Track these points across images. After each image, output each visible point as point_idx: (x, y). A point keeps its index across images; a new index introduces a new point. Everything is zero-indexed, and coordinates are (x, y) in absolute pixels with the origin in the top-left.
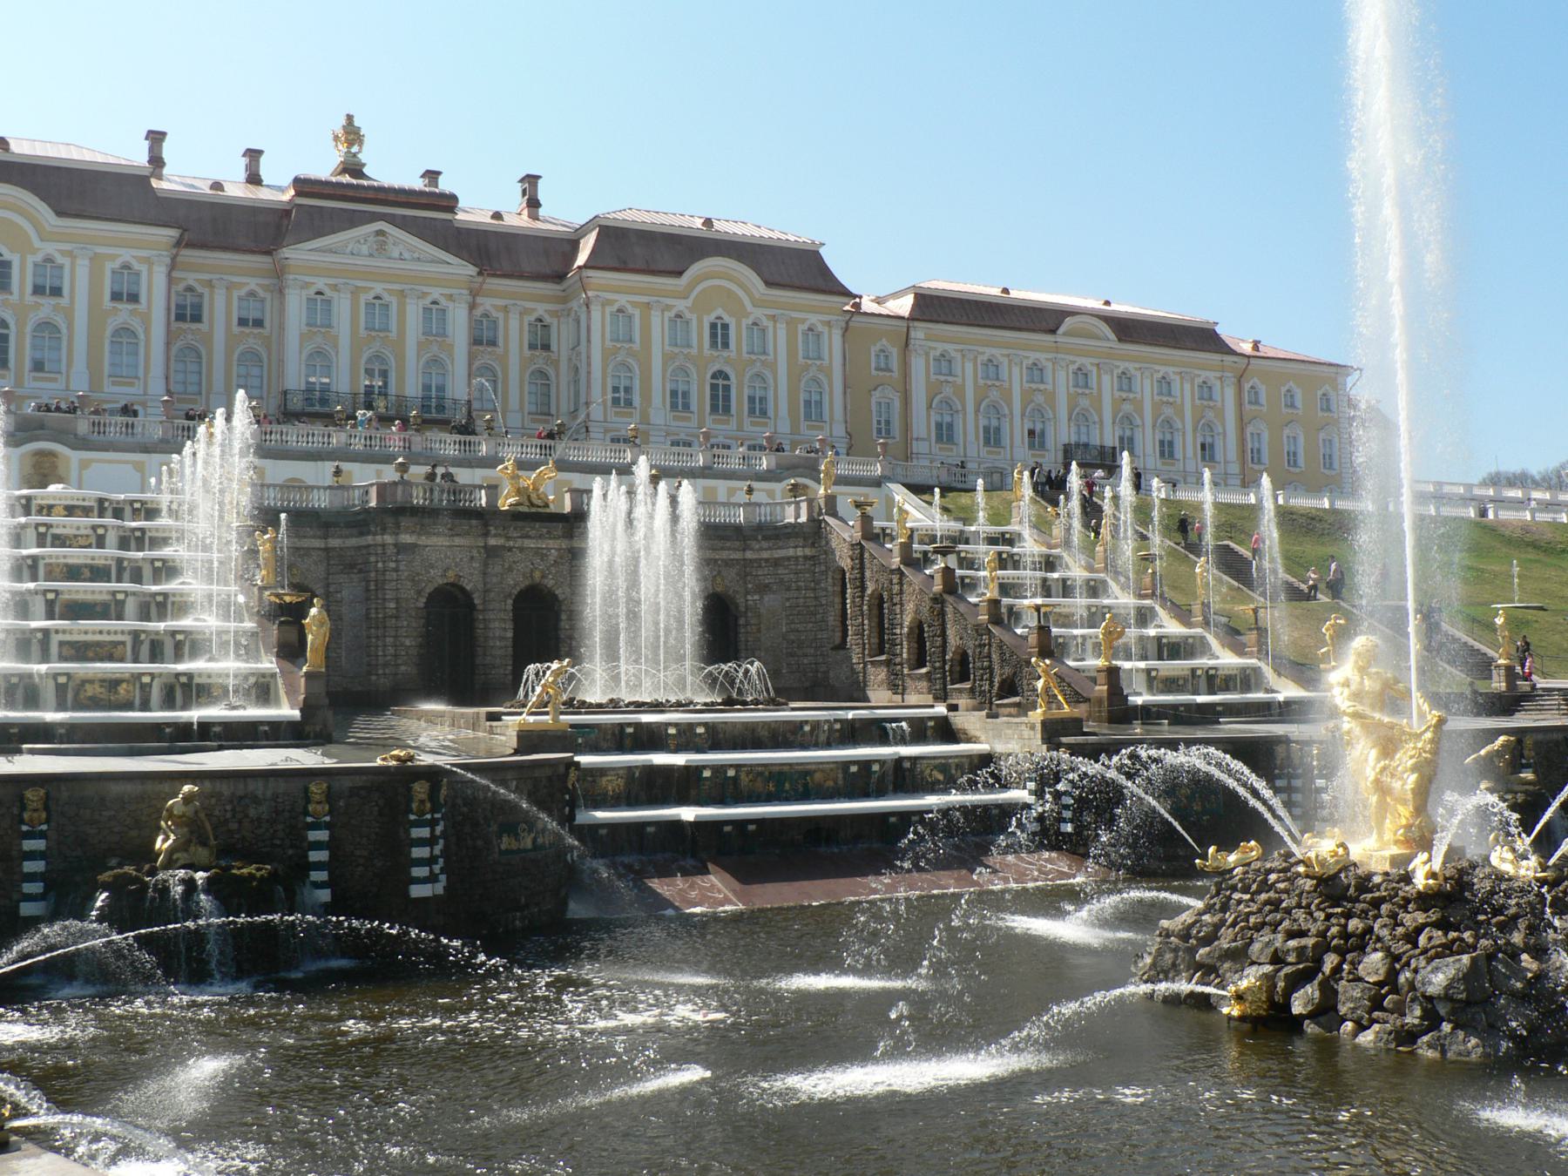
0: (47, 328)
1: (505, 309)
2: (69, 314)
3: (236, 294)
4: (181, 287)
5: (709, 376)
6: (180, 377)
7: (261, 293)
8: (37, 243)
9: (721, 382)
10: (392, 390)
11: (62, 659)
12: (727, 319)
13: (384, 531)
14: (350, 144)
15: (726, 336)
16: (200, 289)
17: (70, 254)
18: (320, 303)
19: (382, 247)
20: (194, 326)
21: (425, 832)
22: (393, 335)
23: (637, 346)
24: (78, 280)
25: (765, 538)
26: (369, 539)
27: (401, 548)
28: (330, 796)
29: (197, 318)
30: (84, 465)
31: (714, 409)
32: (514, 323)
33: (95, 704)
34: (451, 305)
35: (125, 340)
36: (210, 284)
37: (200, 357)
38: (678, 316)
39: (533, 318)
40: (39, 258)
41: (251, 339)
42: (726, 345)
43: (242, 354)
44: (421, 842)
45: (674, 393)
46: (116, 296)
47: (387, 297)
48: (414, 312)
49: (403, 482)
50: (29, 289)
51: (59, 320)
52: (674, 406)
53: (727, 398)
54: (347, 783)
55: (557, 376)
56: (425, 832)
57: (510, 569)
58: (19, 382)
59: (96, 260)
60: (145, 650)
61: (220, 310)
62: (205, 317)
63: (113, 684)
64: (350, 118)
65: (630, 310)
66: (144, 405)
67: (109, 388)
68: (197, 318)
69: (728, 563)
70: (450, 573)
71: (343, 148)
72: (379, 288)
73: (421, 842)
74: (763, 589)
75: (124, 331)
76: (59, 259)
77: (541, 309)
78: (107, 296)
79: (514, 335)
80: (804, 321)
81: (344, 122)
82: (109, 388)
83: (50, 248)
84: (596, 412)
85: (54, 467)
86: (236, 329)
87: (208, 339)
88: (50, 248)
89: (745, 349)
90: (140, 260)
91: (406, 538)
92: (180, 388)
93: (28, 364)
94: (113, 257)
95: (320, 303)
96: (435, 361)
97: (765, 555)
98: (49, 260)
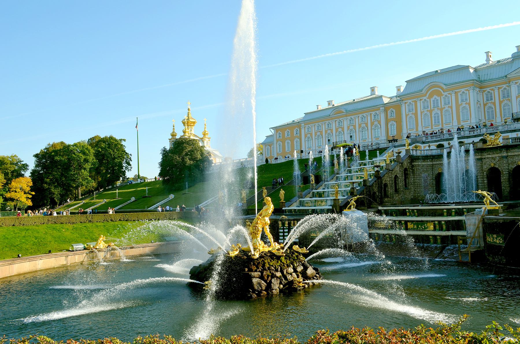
2: (451, 107)
8: (443, 93)
21: (282, 231)
43: (504, 106)
44: (281, 232)
50: (443, 104)
56: (282, 231)
57: (485, 164)
73: (281, 232)
76: (448, 95)
78: (460, 101)
82: (462, 124)
83: (446, 93)
87: (494, 104)
90: (466, 90)
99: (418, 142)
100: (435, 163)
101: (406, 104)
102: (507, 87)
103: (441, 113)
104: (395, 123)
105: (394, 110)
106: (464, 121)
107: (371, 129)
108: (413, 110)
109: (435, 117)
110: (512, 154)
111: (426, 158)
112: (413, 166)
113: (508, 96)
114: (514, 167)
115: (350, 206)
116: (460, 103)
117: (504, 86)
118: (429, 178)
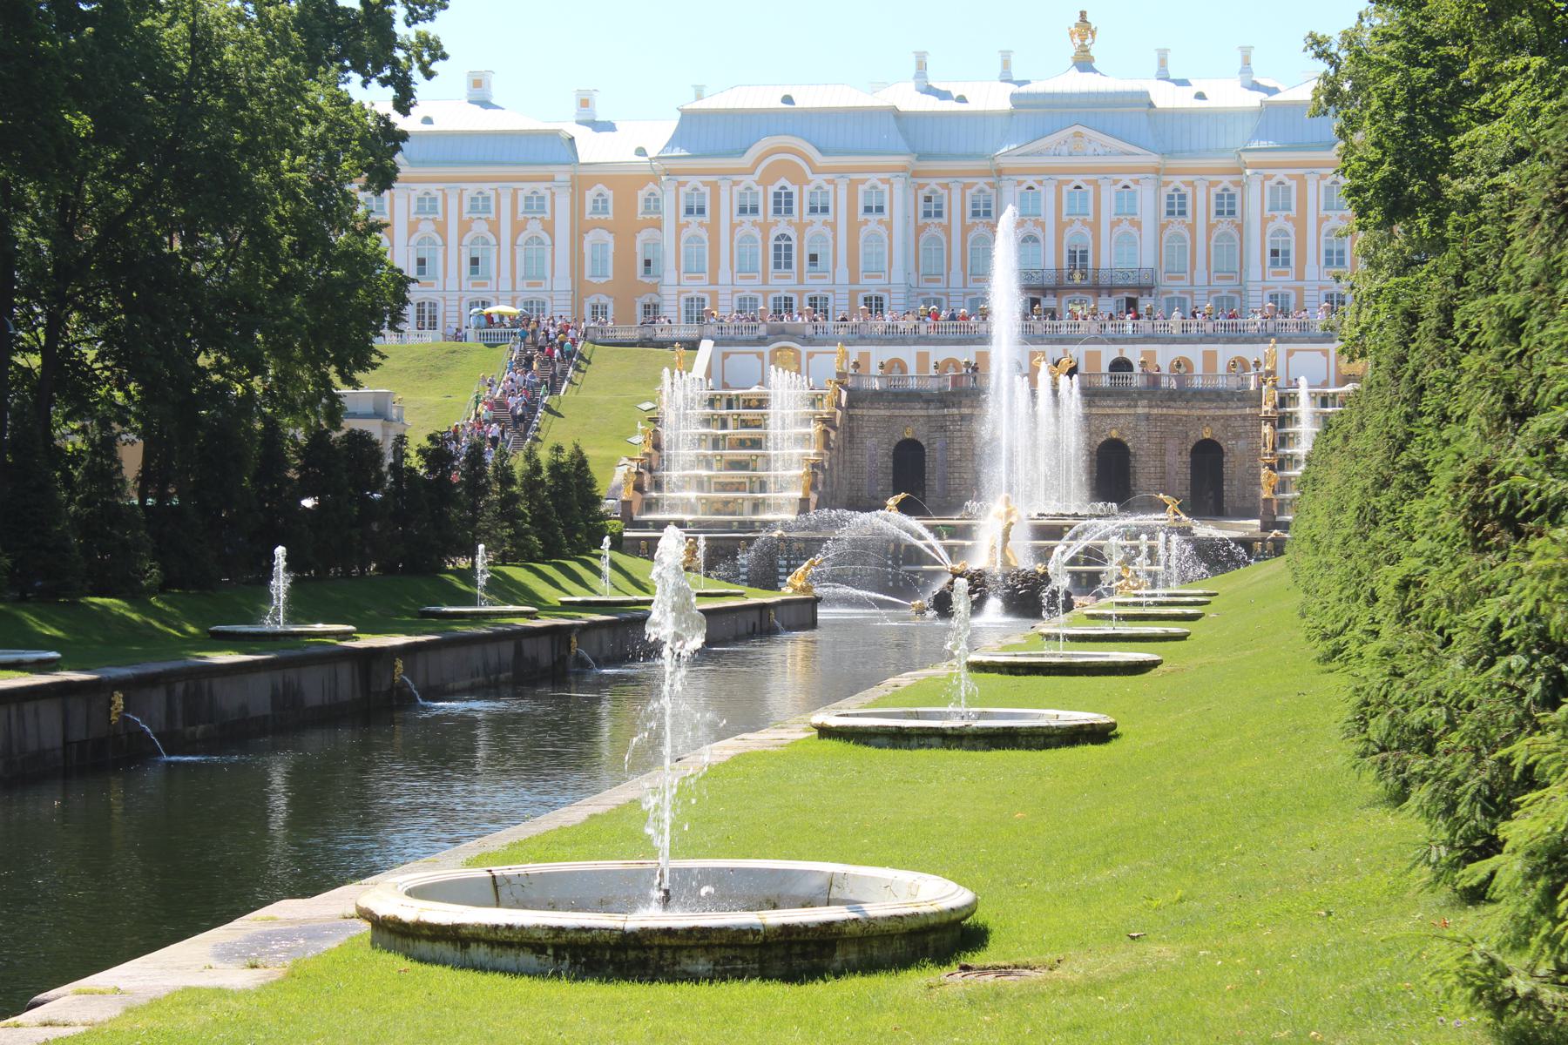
1: (1191, 184)
2: (834, 226)
3: (968, 192)
4: (926, 191)
10: (1090, 264)
16: (940, 191)
17: (829, 182)
20: (937, 220)
22: (1090, 218)
23: (1293, 213)
29: (939, 214)
30: (810, 355)
34: (1138, 188)
36: (946, 187)
39: (1218, 190)
40: (811, 187)
45: (1329, 252)
46: (868, 209)
48: (1108, 194)
50: (806, 208)
52: (1329, 262)
58: (801, 282)
59: (853, 186)
60: (757, 486)
63: (726, 503)
64: (1083, 14)
65: (1288, 182)
66: (889, 291)
67: (863, 281)
68: (939, 214)
69: (1214, 418)
71: (1077, 40)
72: (1078, 180)
74: (1237, 436)
76: (826, 187)
77: (1226, 181)
78: (861, 209)
79: (1201, 203)
81: (1077, 19)
83: (819, 179)
84: (1254, 273)
86: (969, 221)
87: (947, 230)
90: (884, 181)
91: (965, 411)
94: (863, 182)
97: (1239, 412)
98: (819, 187)
100: (897, 412)
101: (682, 190)
102: (986, 188)
103: (800, 239)
107: (514, 244)
108: (701, 211)
109: (777, 248)
110: (1101, 411)
111: (877, 397)
112: (851, 418)
113: (987, 214)
116: (861, 216)
117: (981, 183)
118: (880, 452)
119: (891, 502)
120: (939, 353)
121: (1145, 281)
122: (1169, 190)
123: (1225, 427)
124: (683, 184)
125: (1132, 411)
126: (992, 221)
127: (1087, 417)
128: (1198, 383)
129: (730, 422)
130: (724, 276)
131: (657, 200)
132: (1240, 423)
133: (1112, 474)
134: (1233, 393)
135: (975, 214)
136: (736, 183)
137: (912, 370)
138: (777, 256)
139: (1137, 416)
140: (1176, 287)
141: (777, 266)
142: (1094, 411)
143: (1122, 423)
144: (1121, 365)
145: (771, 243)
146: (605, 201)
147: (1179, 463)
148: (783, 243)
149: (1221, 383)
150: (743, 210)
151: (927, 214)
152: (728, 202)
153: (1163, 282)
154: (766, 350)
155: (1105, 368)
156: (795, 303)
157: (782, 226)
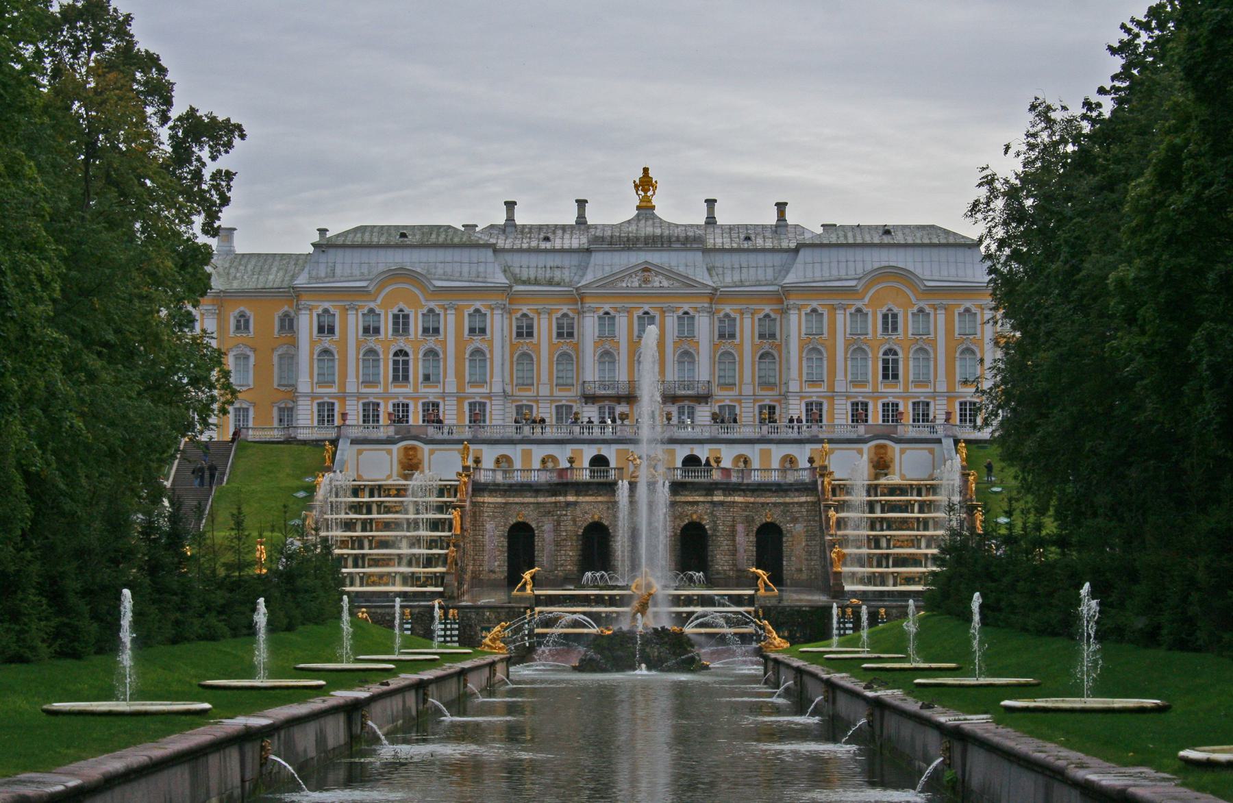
0: (431, 354)
2: (444, 342)
3: (554, 317)
5: (880, 354)
6: (520, 374)
7: (571, 315)
9: (890, 357)
11: (370, 566)
12: (895, 310)
13: (560, 495)
14: (646, 191)
15: (895, 323)
16: (531, 315)
18: (607, 318)
19: (646, 281)
24: (449, 323)
25: (797, 490)
26: (553, 499)
27: (568, 504)
28: (411, 614)
29: (530, 334)
31: (885, 376)
32: (747, 322)
33: (374, 584)
35: (478, 358)
37: (532, 360)
38: (859, 310)
39: (761, 316)
41: (565, 346)
42: (895, 329)
43: (560, 355)
47: (652, 313)
49: (571, 468)
51: (438, 348)
53: (895, 369)
54: (417, 610)
55: (780, 356)
61: (544, 328)
62: (535, 334)
63: (381, 576)
64: (646, 170)
69: (775, 504)
70: (596, 517)
72: (646, 308)
74: (795, 520)
75: (477, 351)
77: (767, 309)
78: (466, 331)
79: (747, 329)
80: (959, 306)
84: (794, 387)
85: (415, 456)
86: (555, 341)
87: (539, 344)
88: (432, 305)
89: (910, 332)
91: (571, 499)
92: (520, 381)
93: (421, 378)
95: (607, 318)
96: (686, 353)
97: (796, 500)
98: (431, 311)
99: (416, 438)
100: (511, 500)
103: (416, 353)
104: (252, 354)
105: (248, 313)
106: (473, 384)
109: (396, 363)
110: (683, 499)
111: (493, 488)
113: (571, 335)
114: (682, 524)
115: (523, 588)
119: (527, 576)
120: (539, 452)
121: (702, 391)
122: (721, 315)
123: (784, 513)
124: (317, 307)
125: (709, 499)
126: (575, 341)
127: (673, 504)
128: (756, 477)
129: (374, 508)
130: (351, 388)
131: (291, 321)
132: (796, 509)
133: (692, 548)
134: (791, 485)
135: (560, 335)
136: (363, 307)
137: (518, 464)
138: (396, 370)
139: (712, 502)
140: (724, 397)
141: (396, 378)
142: (678, 498)
143: (699, 508)
144: (691, 461)
145: (391, 356)
146: (247, 321)
147: (745, 542)
148: (401, 358)
149: (775, 477)
150: (366, 330)
151: (519, 335)
152: (354, 323)
153: (716, 391)
154: (395, 448)
155: (679, 464)
156: (411, 408)
157: (401, 343)
